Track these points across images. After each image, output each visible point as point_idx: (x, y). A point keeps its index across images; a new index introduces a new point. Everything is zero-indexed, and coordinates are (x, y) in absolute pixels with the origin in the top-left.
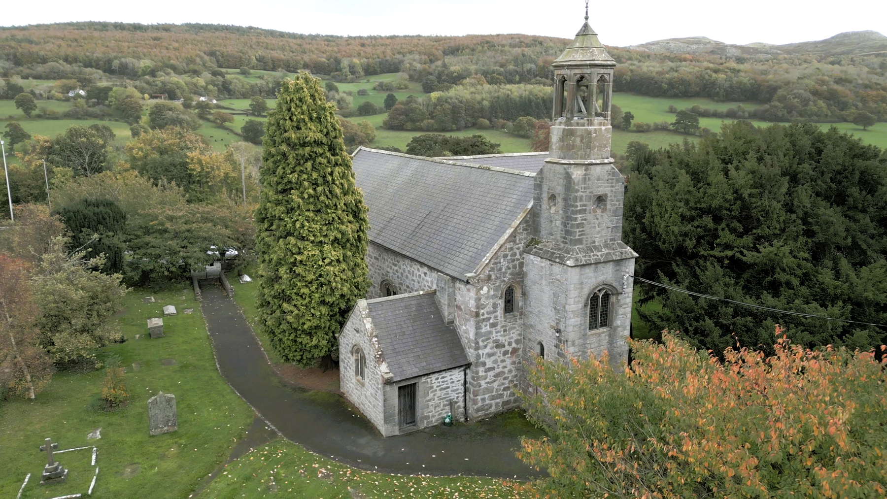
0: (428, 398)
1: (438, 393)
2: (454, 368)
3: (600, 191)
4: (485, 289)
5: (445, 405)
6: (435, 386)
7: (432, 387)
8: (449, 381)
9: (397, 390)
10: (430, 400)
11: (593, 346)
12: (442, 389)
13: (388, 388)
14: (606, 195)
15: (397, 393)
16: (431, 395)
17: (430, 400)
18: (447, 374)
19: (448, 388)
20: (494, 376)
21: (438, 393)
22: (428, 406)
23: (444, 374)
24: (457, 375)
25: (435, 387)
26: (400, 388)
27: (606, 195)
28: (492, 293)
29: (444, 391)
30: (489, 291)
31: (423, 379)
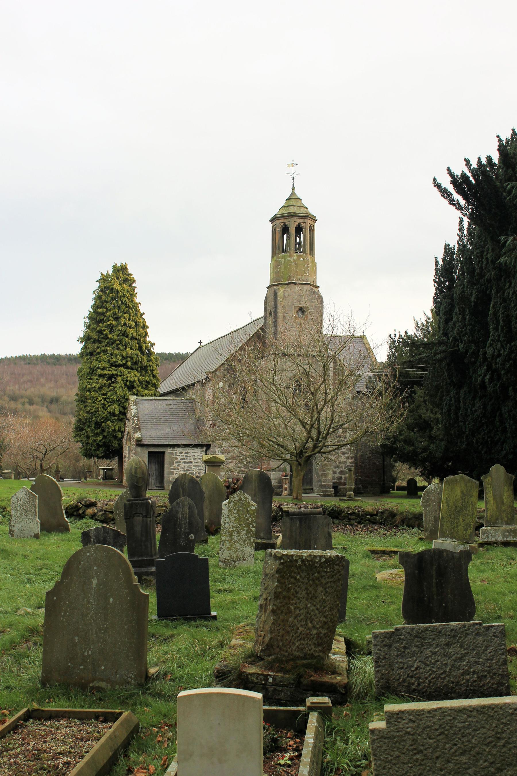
1: (182, 465)
2: (196, 446)
3: (303, 305)
4: (221, 384)
6: (179, 458)
7: (177, 459)
9: (147, 453)
10: (174, 469)
12: (185, 462)
13: (139, 449)
14: (307, 308)
15: (147, 456)
16: (175, 465)
17: (174, 469)
18: (190, 450)
19: (191, 462)
20: (230, 458)
21: (182, 465)
22: (172, 473)
23: (187, 450)
24: (199, 454)
25: (179, 459)
26: (150, 453)
28: (227, 388)
29: (188, 465)
30: (224, 386)
31: (169, 450)
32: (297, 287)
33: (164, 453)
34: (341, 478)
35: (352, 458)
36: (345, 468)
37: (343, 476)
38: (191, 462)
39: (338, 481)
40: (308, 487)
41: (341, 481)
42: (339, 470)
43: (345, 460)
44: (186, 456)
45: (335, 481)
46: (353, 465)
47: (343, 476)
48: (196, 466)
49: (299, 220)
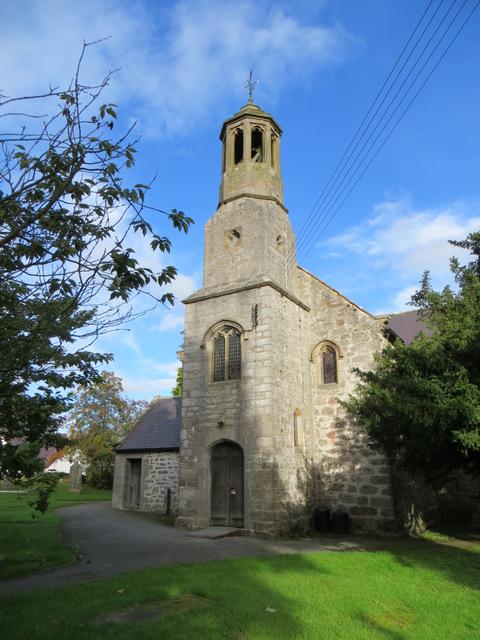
0: (147, 479)
1: (157, 475)
3: (235, 226)
5: (162, 492)
6: (154, 466)
7: (152, 468)
8: (167, 466)
11: (214, 401)
12: (159, 473)
17: (149, 481)
19: (166, 472)
22: (146, 488)
27: (240, 227)
31: (145, 457)
32: (230, 204)
33: (139, 461)
34: (365, 499)
35: (383, 462)
36: (371, 481)
37: (369, 497)
38: (166, 472)
39: (360, 506)
40: (239, 516)
41: (365, 505)
42: (361, 485)
43: (371, 466)
44: (162, 464)
45: (355, 505)
46: (387, 475)
47: (369, 497)
48: (170, 478)
49: (235, 125)
